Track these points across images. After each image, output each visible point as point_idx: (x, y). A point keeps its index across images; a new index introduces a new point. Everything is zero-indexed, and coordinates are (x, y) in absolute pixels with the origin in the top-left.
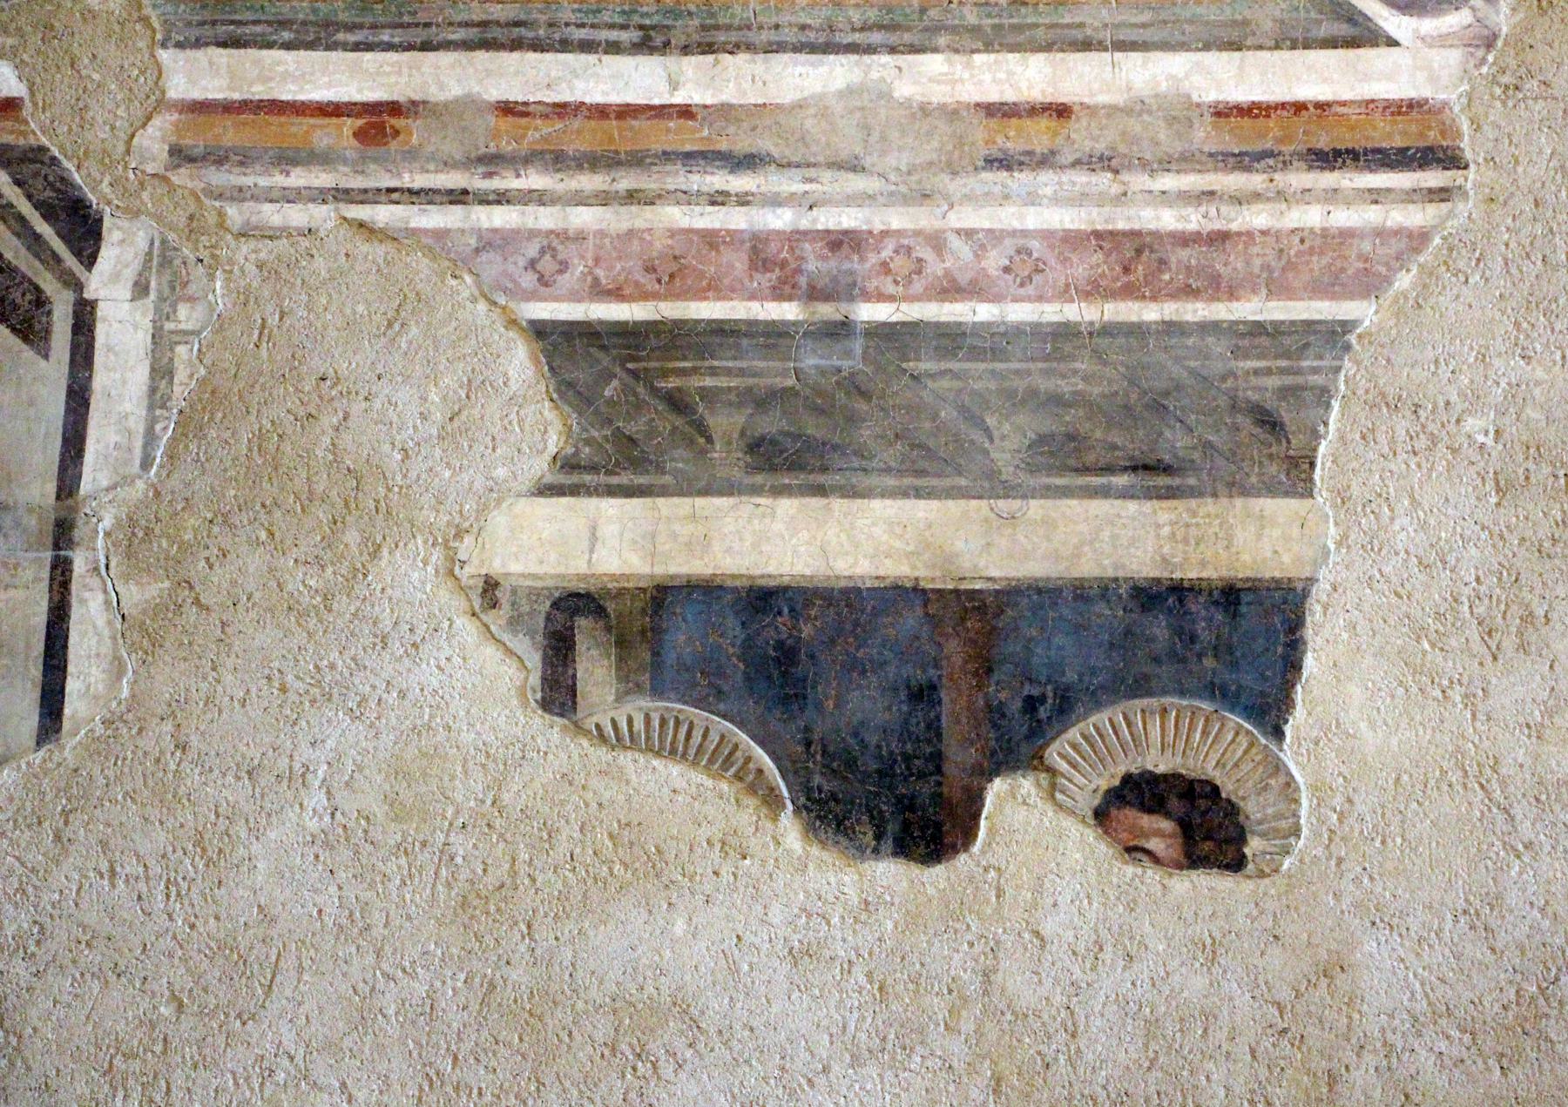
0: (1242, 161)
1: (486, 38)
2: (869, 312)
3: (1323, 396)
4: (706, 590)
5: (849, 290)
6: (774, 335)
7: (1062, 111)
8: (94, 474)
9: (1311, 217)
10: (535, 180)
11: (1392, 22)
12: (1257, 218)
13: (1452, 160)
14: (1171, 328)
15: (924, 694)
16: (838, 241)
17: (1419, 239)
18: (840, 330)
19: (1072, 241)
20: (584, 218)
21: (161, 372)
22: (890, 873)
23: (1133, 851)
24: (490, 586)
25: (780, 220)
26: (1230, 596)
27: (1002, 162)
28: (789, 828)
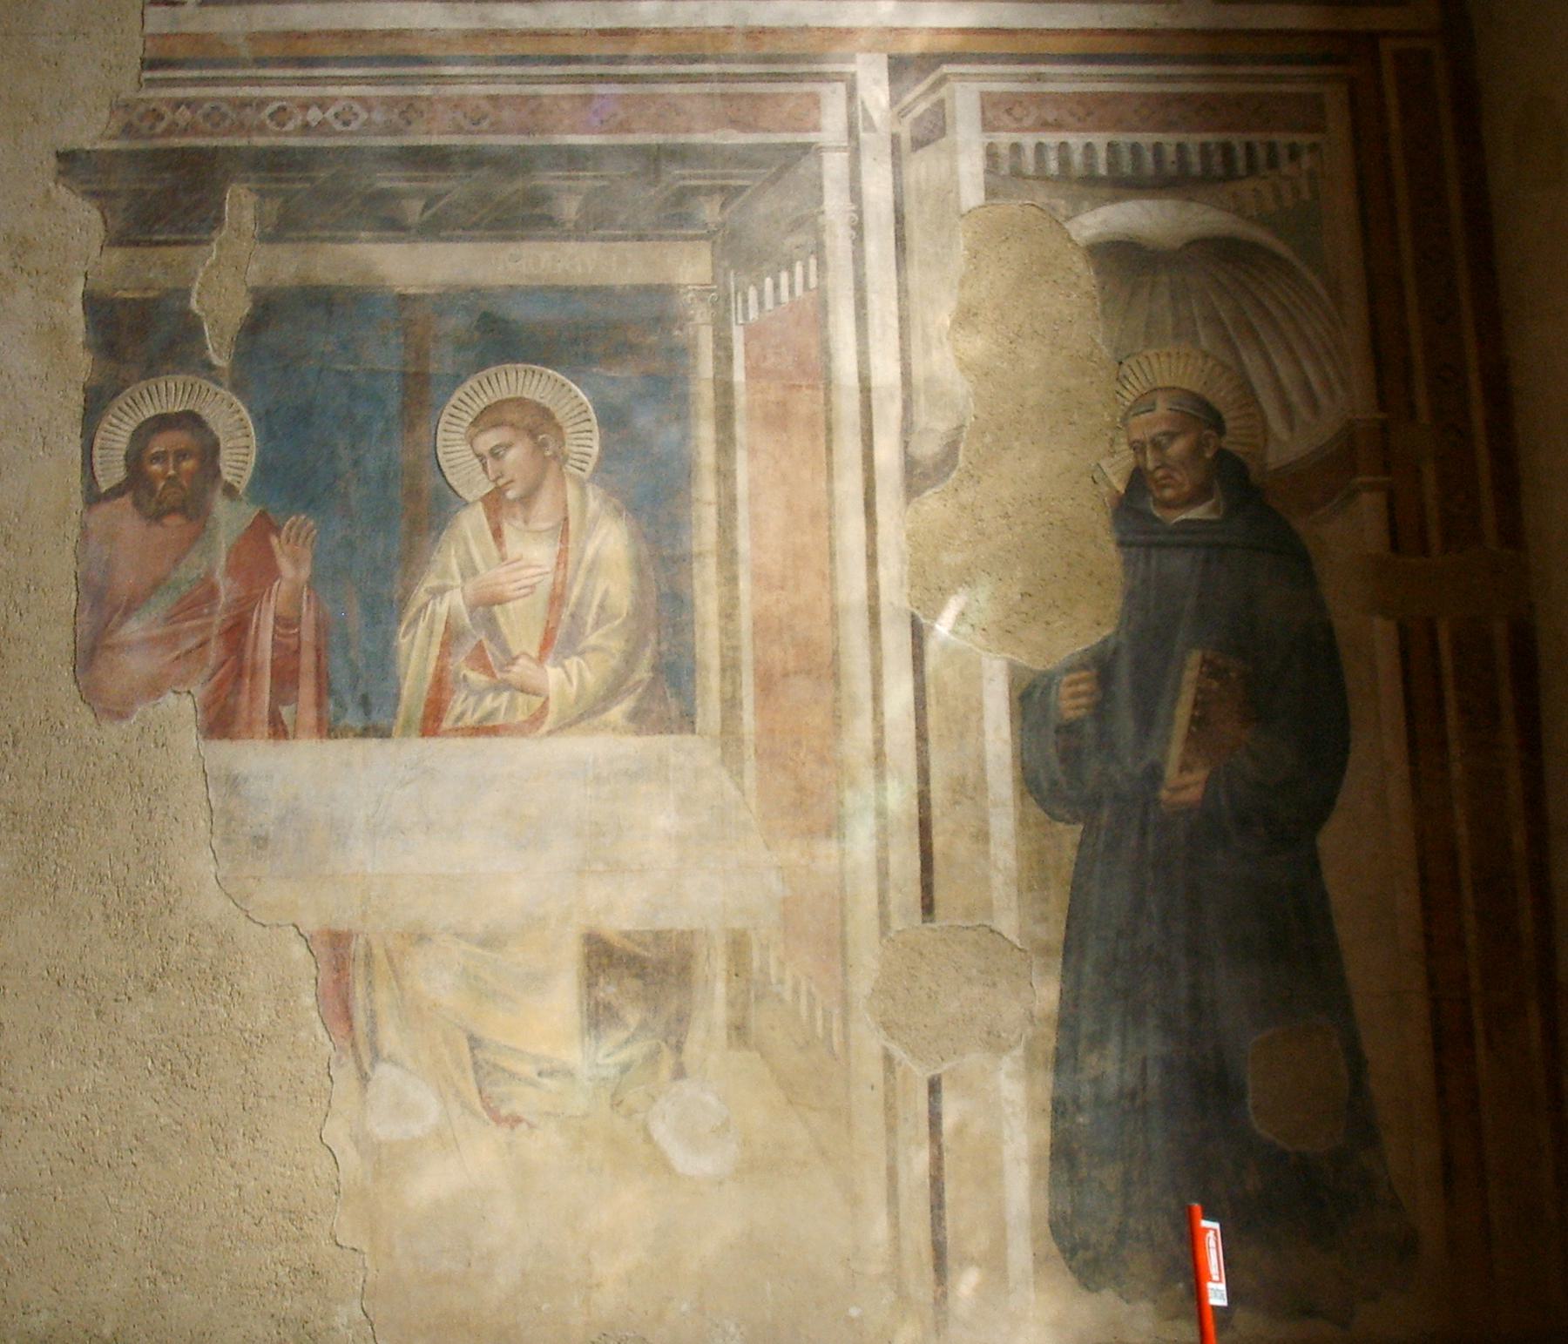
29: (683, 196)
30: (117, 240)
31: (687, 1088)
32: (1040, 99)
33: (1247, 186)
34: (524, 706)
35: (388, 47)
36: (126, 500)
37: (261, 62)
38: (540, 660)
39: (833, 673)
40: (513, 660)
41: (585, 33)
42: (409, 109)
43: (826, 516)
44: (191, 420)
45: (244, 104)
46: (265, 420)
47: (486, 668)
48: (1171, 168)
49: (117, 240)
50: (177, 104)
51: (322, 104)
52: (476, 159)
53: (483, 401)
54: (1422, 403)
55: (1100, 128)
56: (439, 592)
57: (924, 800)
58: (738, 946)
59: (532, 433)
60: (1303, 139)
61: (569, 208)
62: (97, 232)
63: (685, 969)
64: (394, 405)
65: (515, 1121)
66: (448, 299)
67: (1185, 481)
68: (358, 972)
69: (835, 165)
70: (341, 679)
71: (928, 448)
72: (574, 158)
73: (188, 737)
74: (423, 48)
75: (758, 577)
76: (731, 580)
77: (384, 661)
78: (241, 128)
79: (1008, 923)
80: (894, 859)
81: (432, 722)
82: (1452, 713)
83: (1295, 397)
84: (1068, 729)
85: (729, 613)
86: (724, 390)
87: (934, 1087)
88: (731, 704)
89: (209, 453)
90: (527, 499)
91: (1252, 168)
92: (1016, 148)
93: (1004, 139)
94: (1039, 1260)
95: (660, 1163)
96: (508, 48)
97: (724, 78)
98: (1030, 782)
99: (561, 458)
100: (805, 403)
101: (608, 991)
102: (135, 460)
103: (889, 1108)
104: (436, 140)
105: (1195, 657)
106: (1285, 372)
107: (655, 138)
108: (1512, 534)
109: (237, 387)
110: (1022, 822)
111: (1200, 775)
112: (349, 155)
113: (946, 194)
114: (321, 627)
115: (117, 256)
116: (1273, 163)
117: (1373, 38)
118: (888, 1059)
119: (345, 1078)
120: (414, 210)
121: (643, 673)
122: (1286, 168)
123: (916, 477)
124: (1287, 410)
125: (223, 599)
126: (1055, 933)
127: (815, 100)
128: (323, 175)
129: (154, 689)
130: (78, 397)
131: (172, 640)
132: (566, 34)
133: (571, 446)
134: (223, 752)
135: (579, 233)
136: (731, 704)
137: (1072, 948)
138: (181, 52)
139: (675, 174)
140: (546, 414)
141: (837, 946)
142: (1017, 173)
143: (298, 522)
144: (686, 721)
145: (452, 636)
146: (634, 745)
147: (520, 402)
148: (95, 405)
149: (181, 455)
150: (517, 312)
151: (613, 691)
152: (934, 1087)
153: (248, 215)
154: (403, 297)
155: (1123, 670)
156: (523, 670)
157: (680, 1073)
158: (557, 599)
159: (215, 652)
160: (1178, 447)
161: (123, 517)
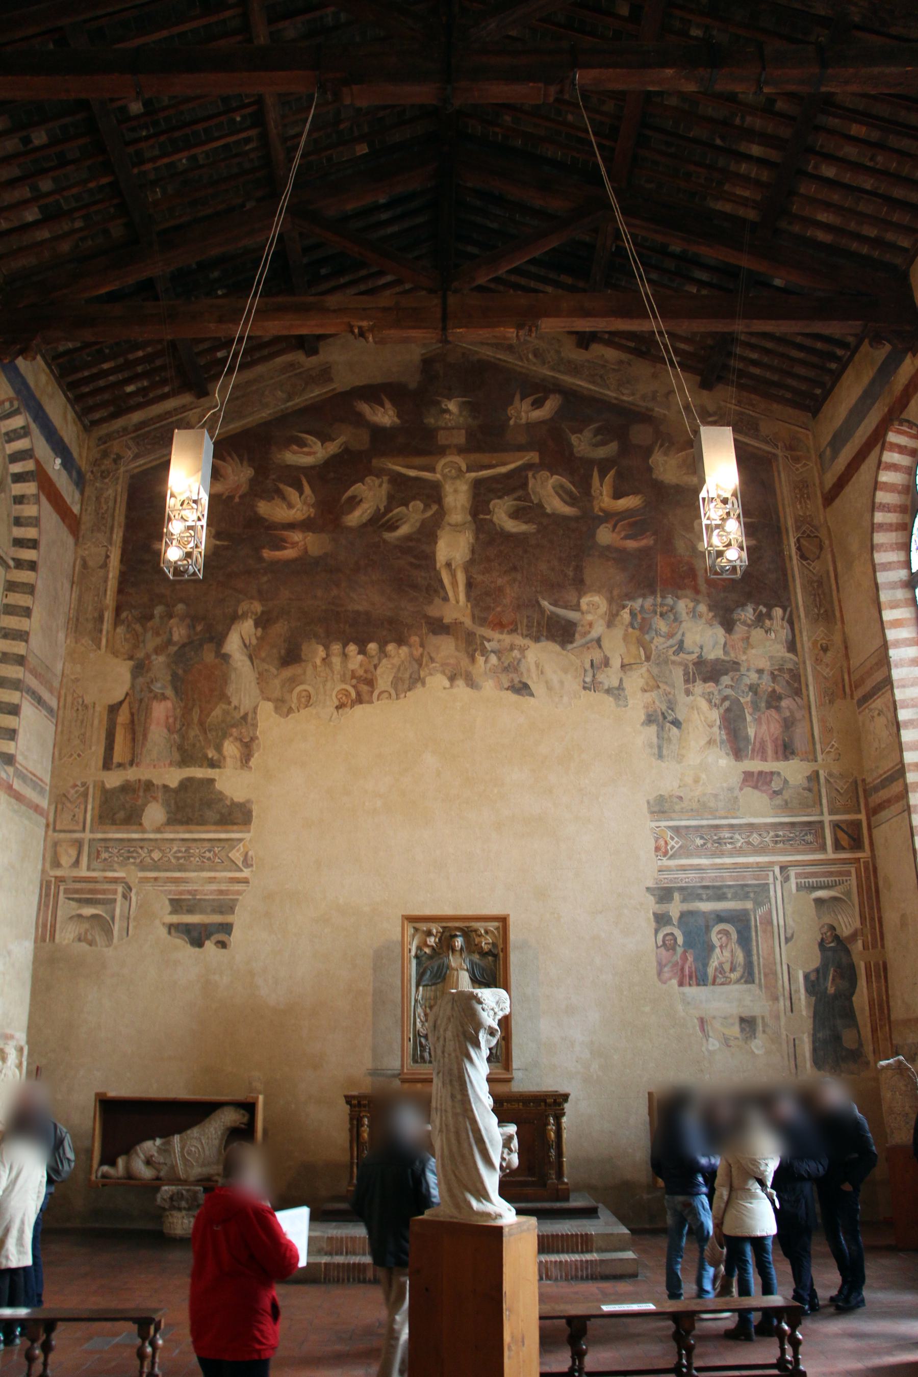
0: (230, 882)
1: (166, 870)
2: (198, 897)
3: (236, 906)
4: (182, 924)
5: (196, 895)
6: (189, 900)
7: (215, 878)
8: (131, 913)
9: (236, 888)
10: (169, 884)
11: (244, 869)
12: (232, 888)
13: (248, 882)
14: (224, 899)
15: (200, 933)
16: (196, 891)
17: (245, 890)
18: (195, 899)
19: (215, 890)
20: (173, 888)
21: (137, 903)
22: (197, 949)
23: (218, 947)
24: (164, 924)
25: (190, 888)
26: (227, 924)
27: (210, 883)
28: (189, 945)
29: (748, 892)
30: (657, 903)
31: (756, 1041)
32: (804, 873)
33: (839, 888)
34: (728, 980)
35: (698, 867)
36: (663, 948)
37: (678, 870)
38: (730, 973)
39: (775, 974)
40: (725, 973)
41: (730, 864)
42: (702, 879)
43: (773, 948)
44: (672, 934)
45: (675, 878)
46: (684, 934)
47: (721, 974)
48: (826, 884)
49: (657, 903)
50: (665, 878)
51: (688, 878)
52: (714, 887)
53: (718, 929)
54: (868, 924)
55: (815, 878)
56: (713, 962)
57: (790, 994)
58: (763, 1018)
59: (726, 935)
60: (848, 878)
61: (729, 896)
62: (654, 902)
63: (755, 1024)
64: (704, 930)
65: (730, 1046)
66: (711, 912)
67: (830, 940)
68: (705, 1024)
69: (772, 887)
70: (699, 977)
71: (789, 935)
72: (730, 887)
73: (676, 986)
74: (703, 867)
75: (764, 958)
76: (759, 958)
77: (705, 974)
78: (675, 883)
79: (804, 1013)
80: (786, 1004)
81: (714, 983)
82: (873, 978)
83: (848, 925)
84: (813, 981)
85: (759, 964)
86: (756, 926)
87: (794, 1040)
88: (760, 979)
89: (675, 940)
90: (726, 946)
91: (840, 884)
92: (801, 882)
93: (799, 880)
94: (812, 1067)
95: (753, 1052)
96: (718, 867)
97: (753, 871)
98: (807, 990)
99: (731, 939)
100: (769, 928)
101: (743, 1025)
102: (664, 941)
103: (787, 1042)
104: (707, 884)
105: (832, 969)
106: (845, 919)
107: (742, 883)
108: (883, 946)
109: (679, 928)
110: (806, 997)
111: (833, 989)
112: (694, 887)
113: (790, 890)
114: (695, 968)
115: (657, 906)
116: (843, 883)
117: (859, 859)
118: (787, 1036)
119: (704, 1040)
120: (704, 897)
121: (746, 974)
122: (845, 884)
123: (787, 940)
124: (846, 926)
125: (680, 964)
126: (811, 1014)
127: (768, 875)
128: (689, 891)
129: (670, 979)
130: (653, 931)
131: (672, 971)
132: (726, 864)
133: (733, 937)
134: (682, 989)
135: (731, 900)
136: (760, 979)
137: (815, 1017)
138: (664, 869)
139: (747, 889)
140: (728, 931)
141: (777, 1017)
142: (801, 887)
143: (690, 951)
144: (753, 982)
145: (716, 969)
146: (745, 986)
147: (724, 930)
148: (657, 932)
149: (671, 940)
150: (723, 914)
151: (742, 977)
152: (794, 1040)
153: (678, 898)
154: (704, 913)
155: (821, 971)
156: (727, 974)
157: (755, 1038)
158: (732, 963)
159: (679, 973)
160: (829, 934)
161: (662, 950)
